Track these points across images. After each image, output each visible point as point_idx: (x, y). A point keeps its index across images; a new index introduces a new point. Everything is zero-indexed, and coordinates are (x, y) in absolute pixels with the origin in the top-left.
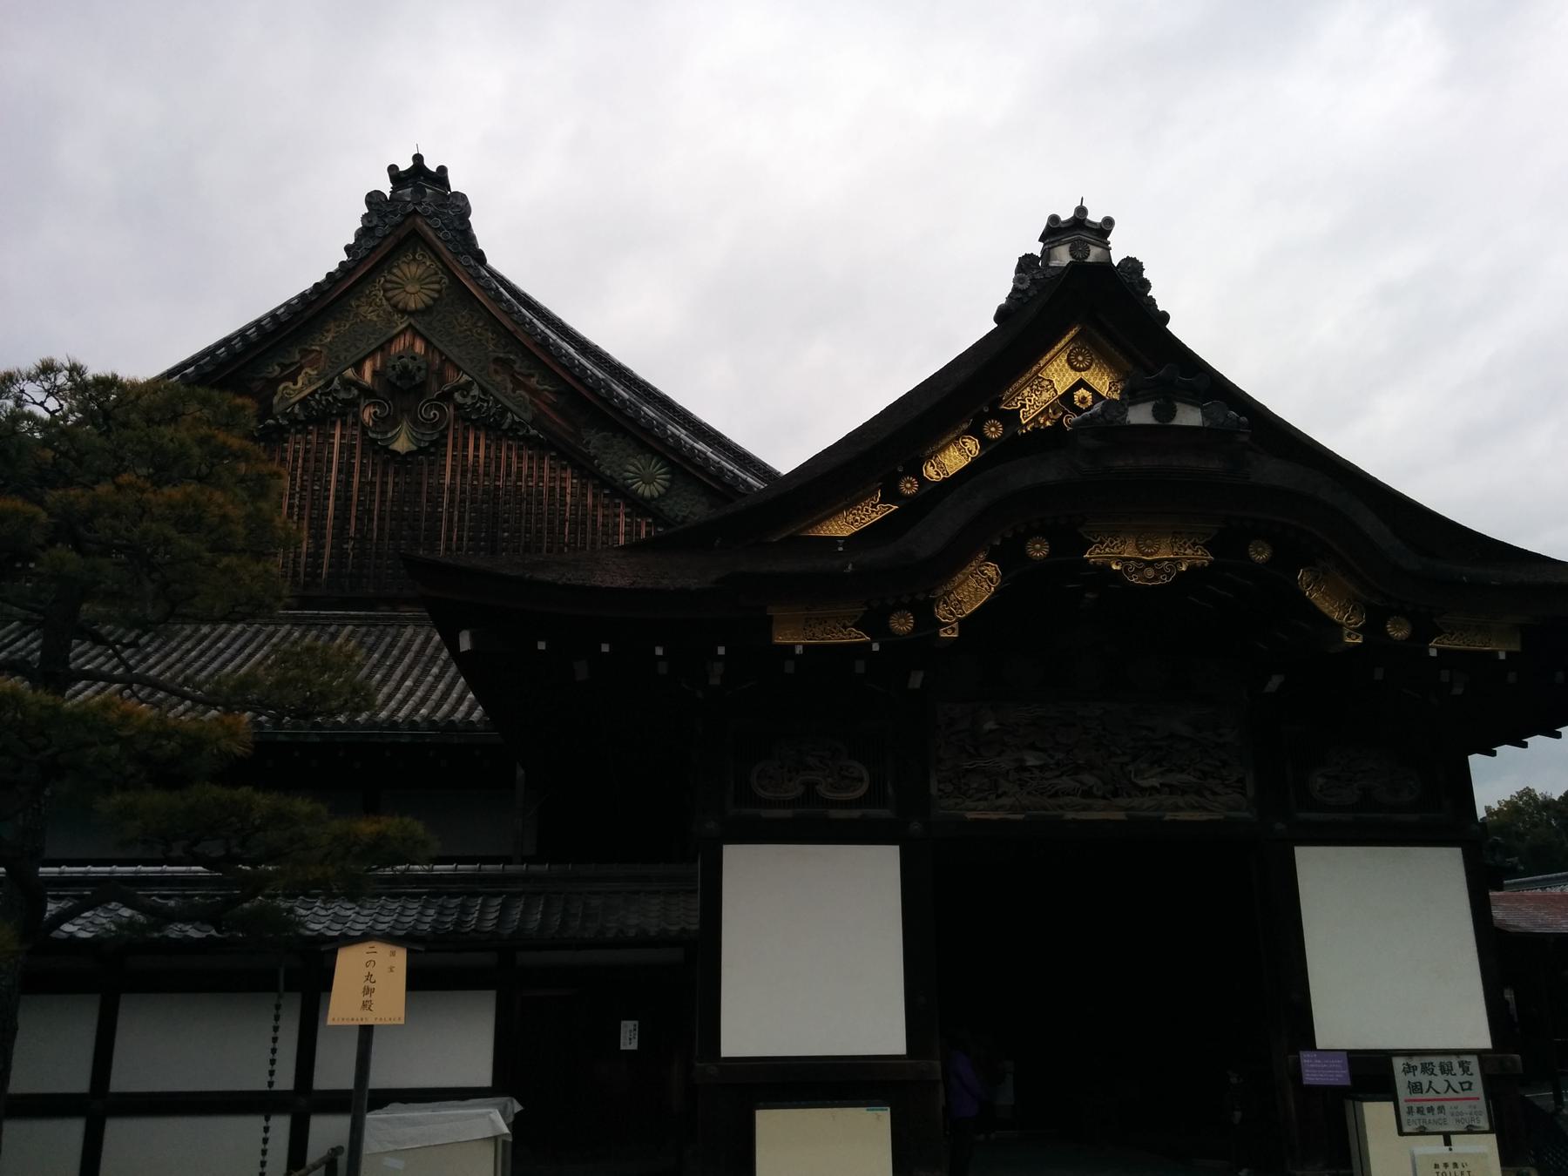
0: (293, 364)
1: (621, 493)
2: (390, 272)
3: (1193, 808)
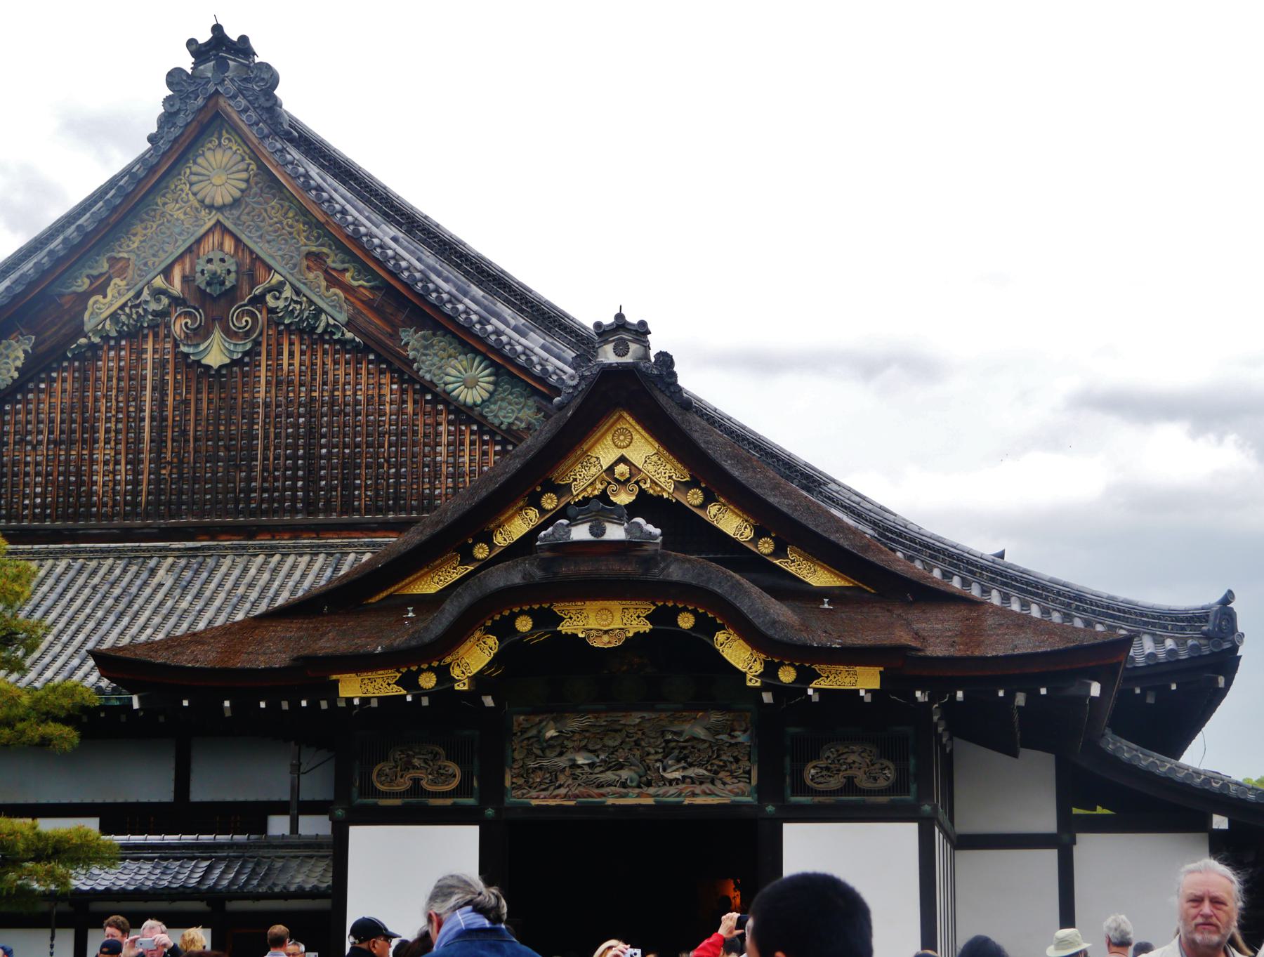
0: (101, 275)
1: (444, 399)
2: (195, 163)
3: (705, 793)
